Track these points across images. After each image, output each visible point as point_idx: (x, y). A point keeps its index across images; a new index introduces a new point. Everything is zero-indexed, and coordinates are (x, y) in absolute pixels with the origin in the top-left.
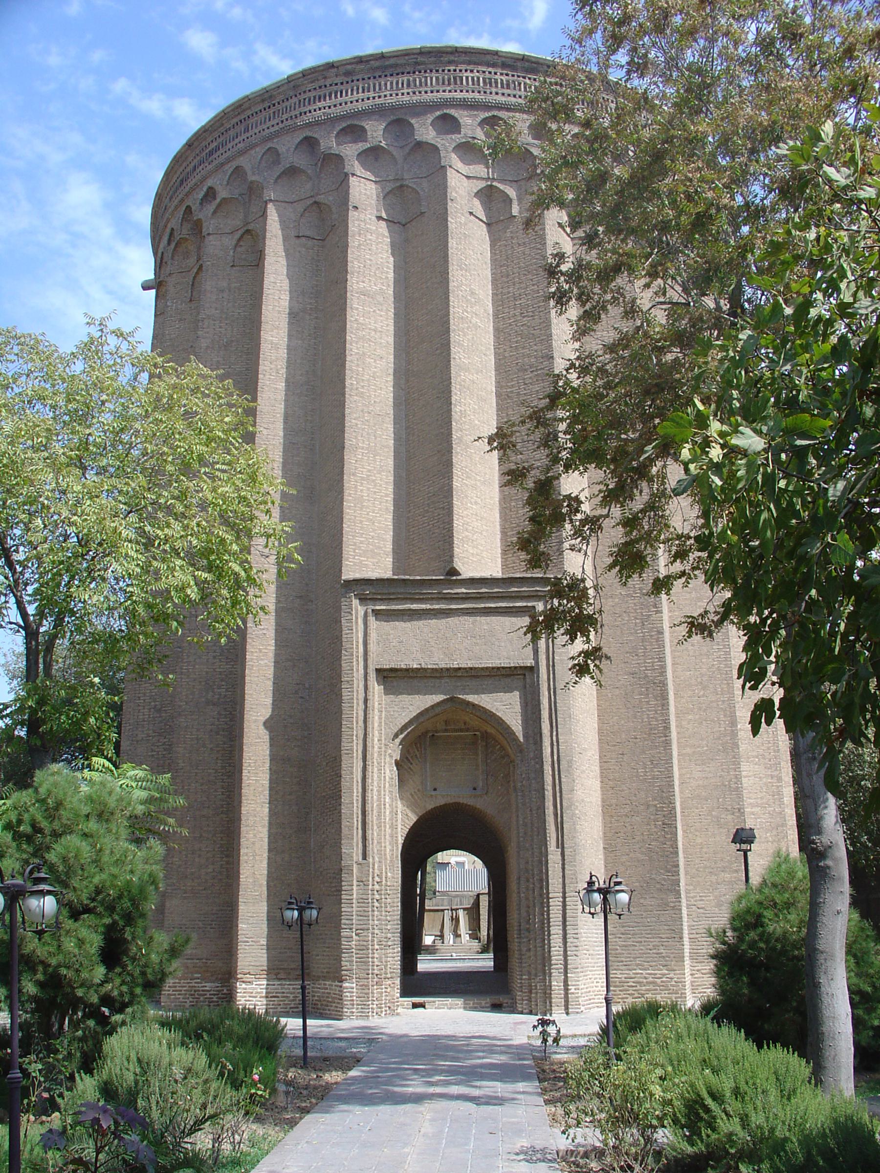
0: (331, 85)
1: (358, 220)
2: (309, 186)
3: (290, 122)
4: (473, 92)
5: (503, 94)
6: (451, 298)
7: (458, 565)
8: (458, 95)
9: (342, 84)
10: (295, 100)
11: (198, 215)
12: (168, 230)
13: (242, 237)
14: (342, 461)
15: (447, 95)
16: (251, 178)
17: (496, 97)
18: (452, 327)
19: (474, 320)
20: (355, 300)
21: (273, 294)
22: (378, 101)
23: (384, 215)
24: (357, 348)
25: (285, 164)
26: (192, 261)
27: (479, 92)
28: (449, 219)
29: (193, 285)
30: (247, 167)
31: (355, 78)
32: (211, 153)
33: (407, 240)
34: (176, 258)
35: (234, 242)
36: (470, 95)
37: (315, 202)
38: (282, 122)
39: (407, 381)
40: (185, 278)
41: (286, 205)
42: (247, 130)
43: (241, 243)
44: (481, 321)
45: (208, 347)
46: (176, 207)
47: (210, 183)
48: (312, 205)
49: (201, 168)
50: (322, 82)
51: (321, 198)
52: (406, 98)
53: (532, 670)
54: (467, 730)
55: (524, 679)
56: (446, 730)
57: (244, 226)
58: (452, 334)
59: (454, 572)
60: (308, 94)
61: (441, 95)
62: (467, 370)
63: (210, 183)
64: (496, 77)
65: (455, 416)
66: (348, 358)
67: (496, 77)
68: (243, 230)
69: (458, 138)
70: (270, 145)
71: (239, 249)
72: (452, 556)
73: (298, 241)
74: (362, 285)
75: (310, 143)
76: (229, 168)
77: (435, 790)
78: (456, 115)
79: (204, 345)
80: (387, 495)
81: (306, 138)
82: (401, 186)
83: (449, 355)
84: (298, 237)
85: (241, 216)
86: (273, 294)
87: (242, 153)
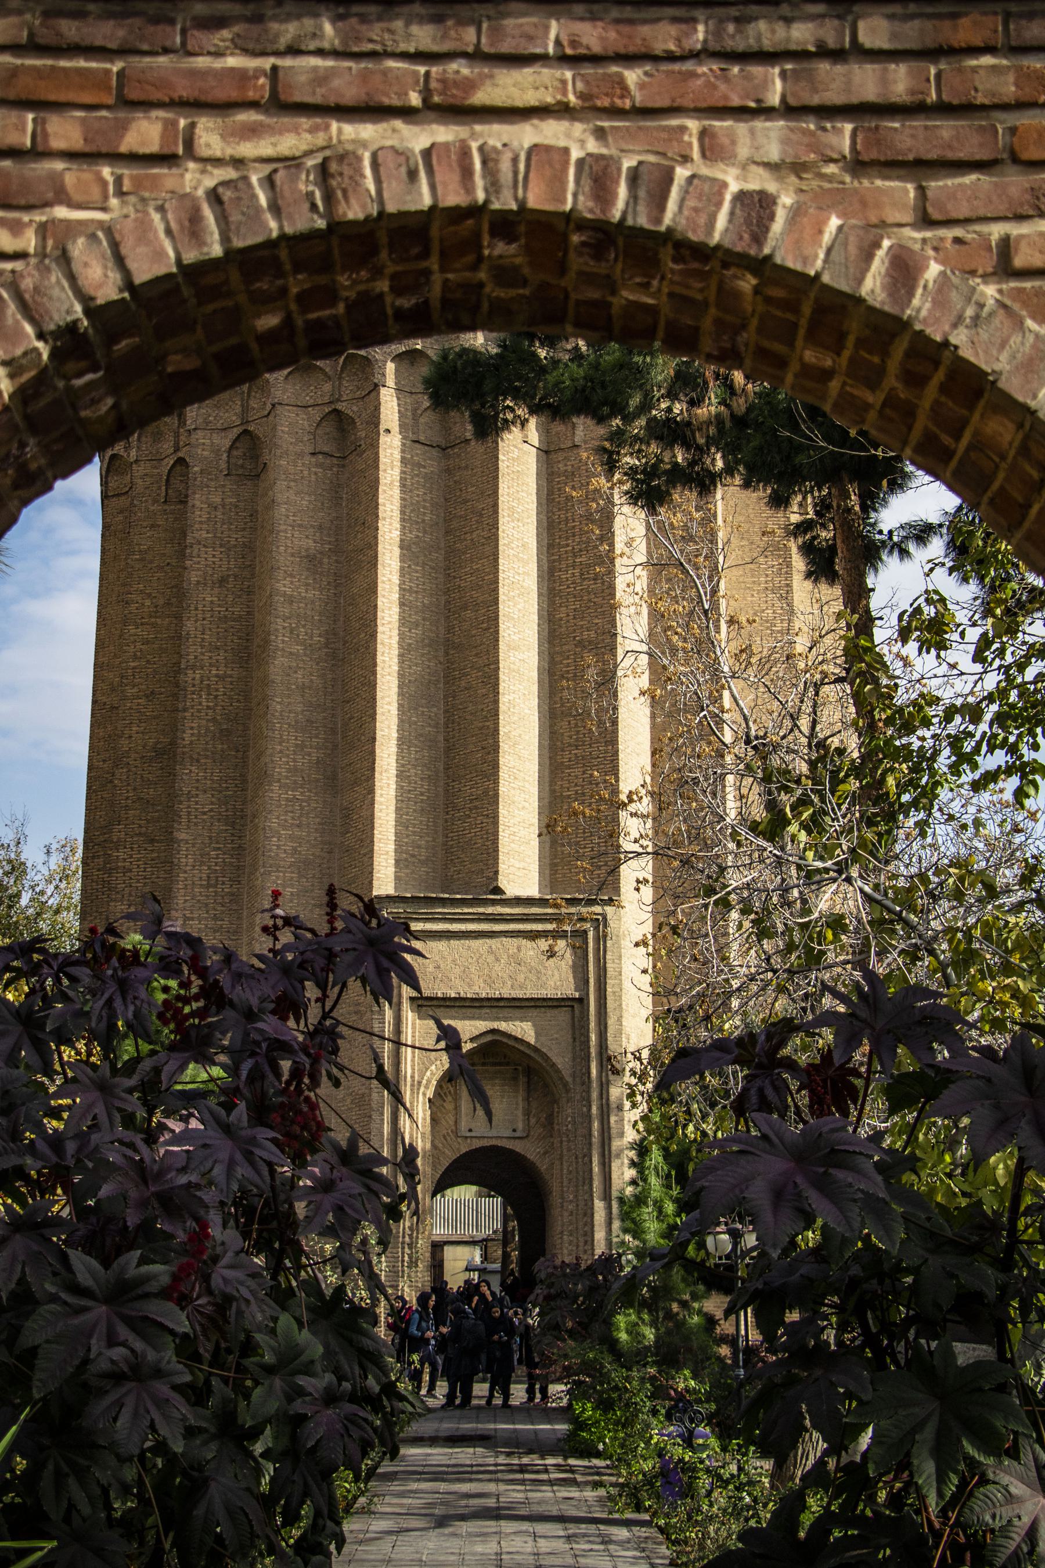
2: (327, 387)
6: (501, 561)
7: (503, 882)
14: (373, 753)
18: (502, 597)
21: (286, 531)
23: (422, 438)
26: (167, 447)
28: (501, 457)
29: (167, 480)
33: (448, 471)
34: (144, 439)
35: (227, 443)
37: (335, 410)
39: (447, 654)
40: (156, 468)
41: (299, 411)
43: (238, 445)
45: (198, 582)
48: (330, 413)
51: (339, 406)
53: (582, 1001)
54: (508, 1064)
55: (573, 1011)
56: (484, 1064)
58: (501, 606)
59: (498, 890)
65: (502, 707)
66: (380, 629)
68: (241, 429)
71: (235, 453)
72: (497, 873)
77: (470, 1130)
79: (194, 579)
80: (422, 794)
83: (497, 632)
84: (313, 454)
85: (238, 409)
86: (286, 531)
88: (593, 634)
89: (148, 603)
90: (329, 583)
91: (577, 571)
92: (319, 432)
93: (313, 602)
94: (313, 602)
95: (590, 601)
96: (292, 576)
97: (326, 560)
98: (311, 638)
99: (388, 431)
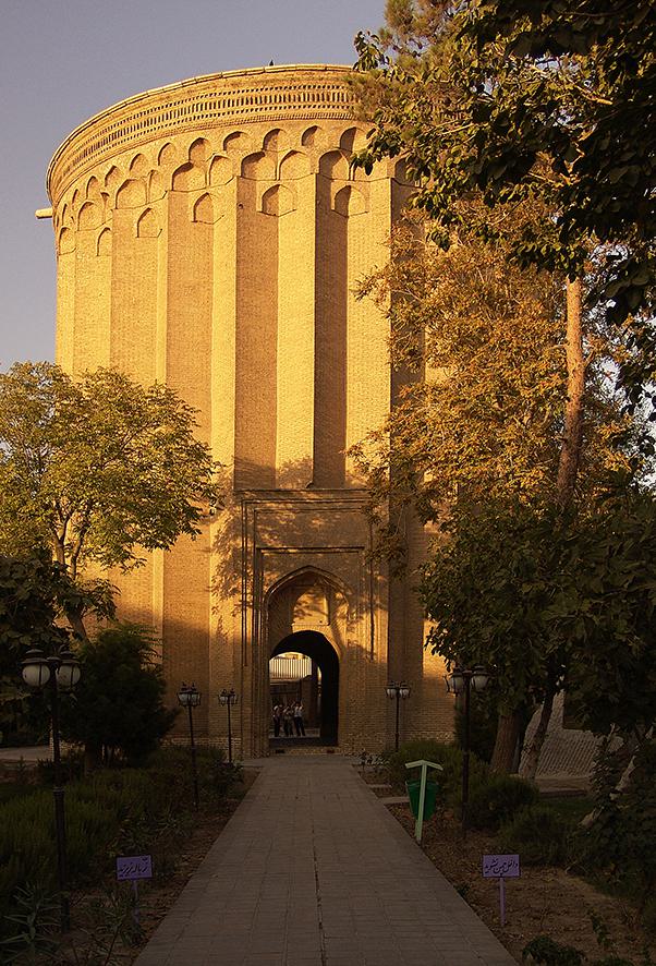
8: (326, 110)
10: (189, 103)
12: (72, 190)
13: (144, 214)
22: (262, 113)
30: (149, 157)
32: (114, 136)
36: (335, 111)
42: (147, 123)
46: (81, 175)
47: (114, 162)
49: (104, 147)
50: (212, 91)
52: (283, 112)
60: (200, 100)
63: (114, 162)
68: (143, 210)
70: (167, 140)
76: (132, 153)
87: (143, 143)
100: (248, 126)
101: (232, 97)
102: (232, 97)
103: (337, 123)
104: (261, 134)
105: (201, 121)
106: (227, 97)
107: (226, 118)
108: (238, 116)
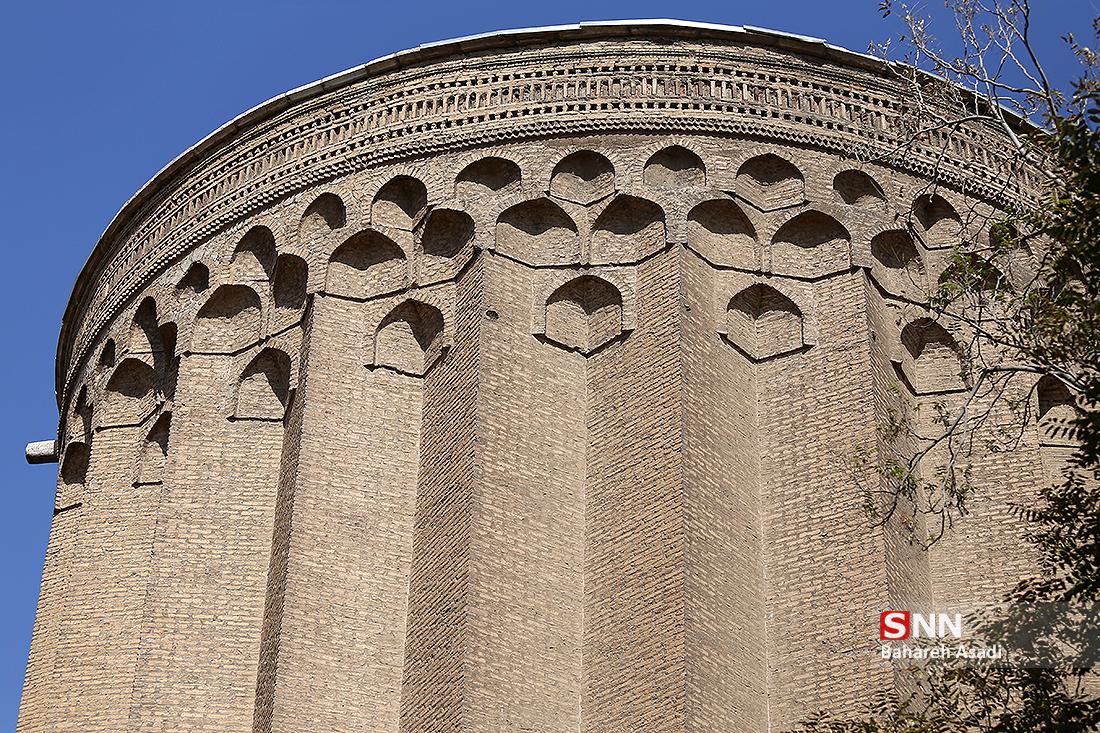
0: (453, 84)
1: (498, 338)
3: (368, 148)
4: (730, 109)
5: (787, 117)
9: (474, 83)
11: (165, 314)
15: (679, 113)
16: (283, 249)
17: (775, 122)
19: (729, 547)
20: (488, 498)
21: (318, 476)
24: (489, 592)
25: (353, 225)
27: (741, 110)
31: (500, 75)
38: (353, 147)
44: (740, 548)
45: (172, 576)
47: (197, 255)
51: (415, 295)
57: (260, 342)
61: (668, 112)
62: (714, 645)
64: (774, 85)
67: (774, 85)
69: (700, 189)
70: (324, 189)
73: (371, 375)
74: (501, 467)
75: (406, 193)
76: (239, 232)
78: (697, 151)
81: (399, 179)
82: (585, 279)
88: (846, 629)
89: (95, 631)
90: (387, 561)
91: (815, 532)
92: (382, 334)
93: (357, 588)
94: (357, 588)
95: (840, 576)
96: (323, 544)
97: (383, 525)
98: (352, 643)
99: (493, 315)
100: (516, 147)
101: (478, 90)
102: (478, 90)
103: (731, 145)
104: (548, 160)
105: (406, 141)
106: (469, 89)
107: (465, 132)
108: (493, 124)
